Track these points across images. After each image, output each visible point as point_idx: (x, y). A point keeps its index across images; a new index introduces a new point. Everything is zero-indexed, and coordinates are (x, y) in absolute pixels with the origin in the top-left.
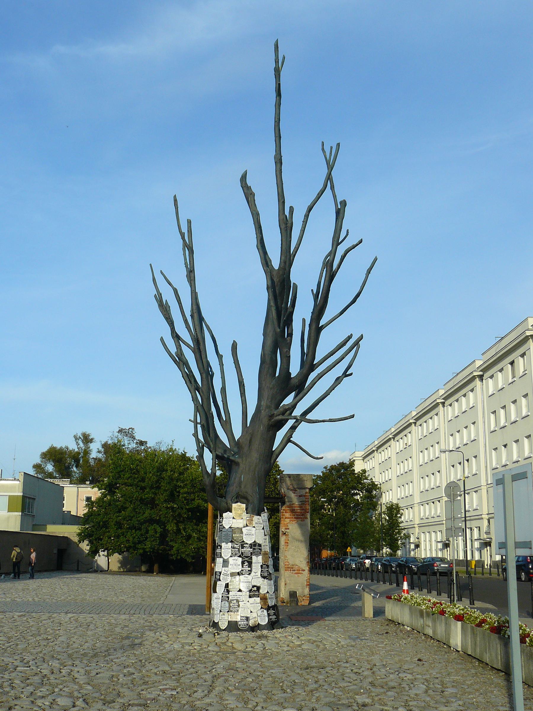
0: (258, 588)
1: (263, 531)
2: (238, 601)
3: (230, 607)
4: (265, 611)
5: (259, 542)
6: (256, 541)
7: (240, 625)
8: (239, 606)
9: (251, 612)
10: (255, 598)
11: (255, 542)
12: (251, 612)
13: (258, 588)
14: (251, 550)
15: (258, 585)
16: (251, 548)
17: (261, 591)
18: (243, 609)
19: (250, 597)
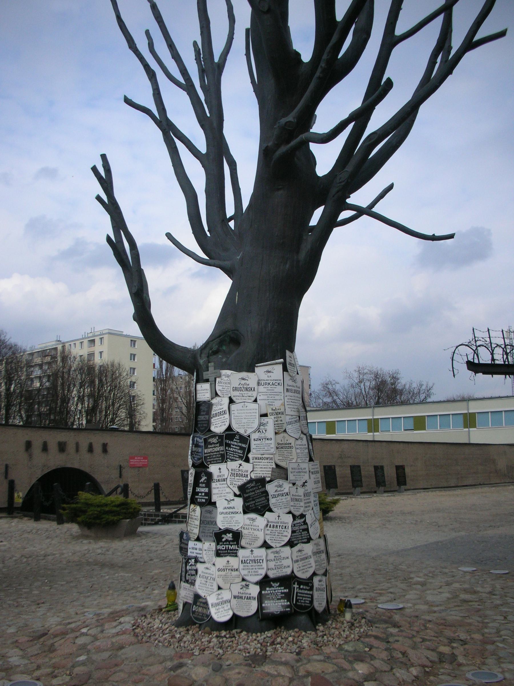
0: (237, 536)
1: (255, 406)
2: (197, 561)
3: (186, 571)
4: (255, 590)
5: (242, 431)
6: (235, 427)
7: (194, 612)
8: (196, 571)
9: (219, 588)
10: (228, 558)
11: (229, 428)
12: (219, 588)
13: (237, 536)
14: (222, 448)
15: (235, 528)
16: (221, 444)
17: (243, 543)
18: (203, 580)
19: (218, 554)
